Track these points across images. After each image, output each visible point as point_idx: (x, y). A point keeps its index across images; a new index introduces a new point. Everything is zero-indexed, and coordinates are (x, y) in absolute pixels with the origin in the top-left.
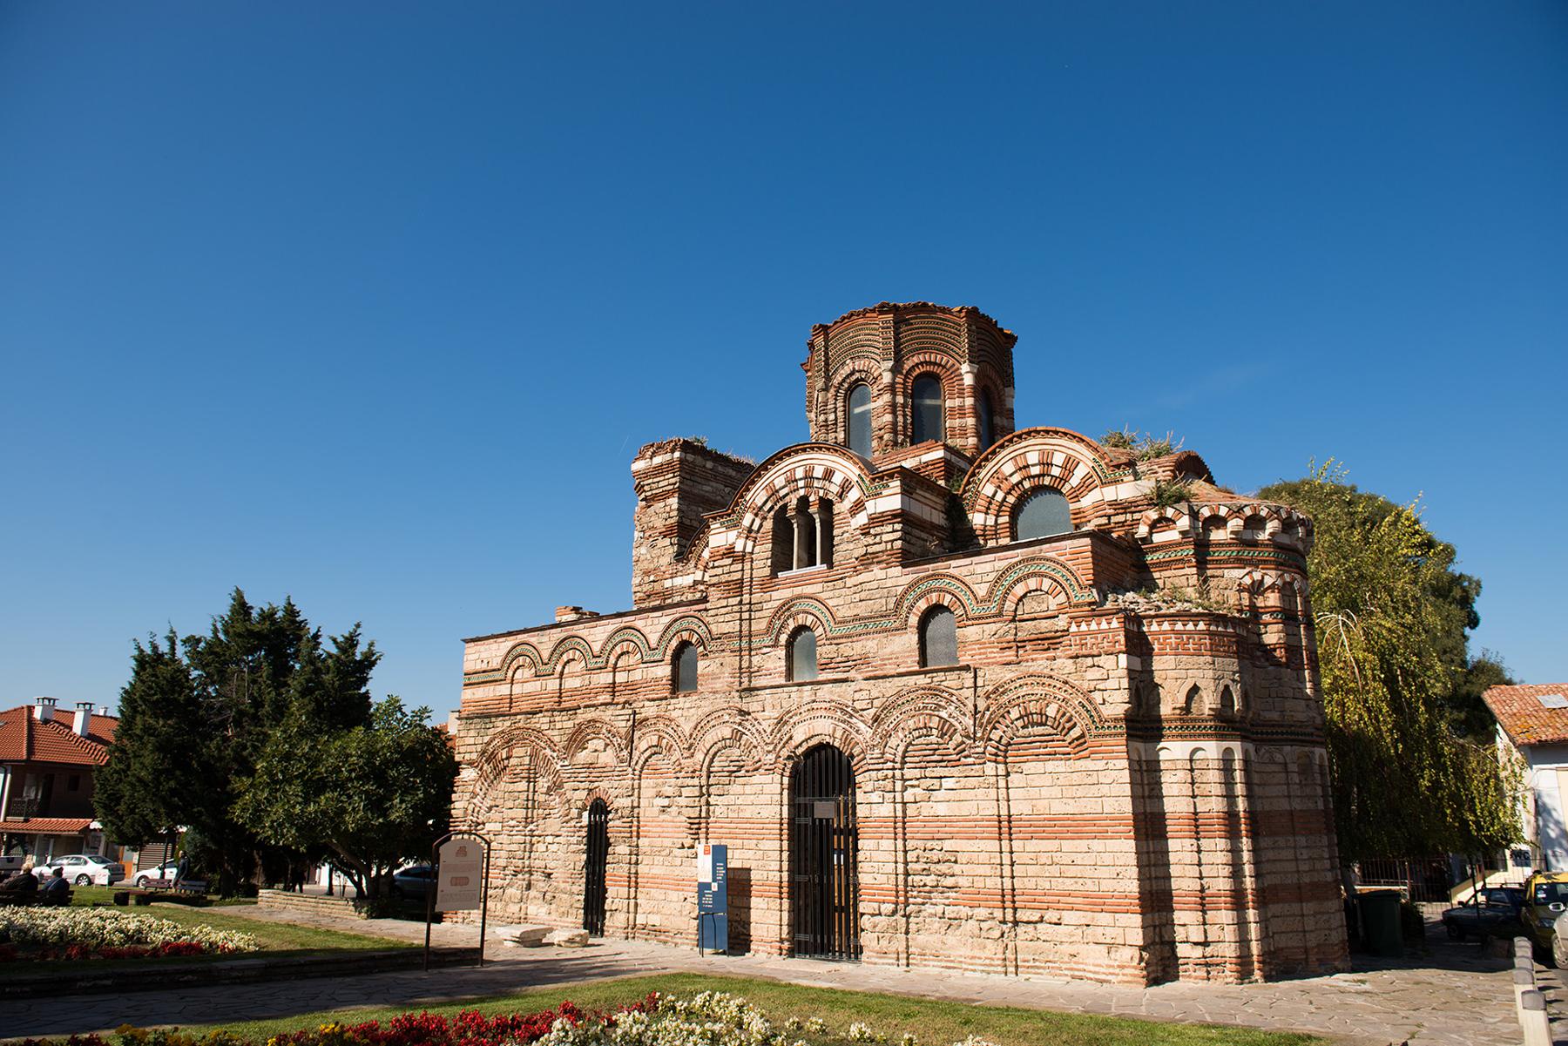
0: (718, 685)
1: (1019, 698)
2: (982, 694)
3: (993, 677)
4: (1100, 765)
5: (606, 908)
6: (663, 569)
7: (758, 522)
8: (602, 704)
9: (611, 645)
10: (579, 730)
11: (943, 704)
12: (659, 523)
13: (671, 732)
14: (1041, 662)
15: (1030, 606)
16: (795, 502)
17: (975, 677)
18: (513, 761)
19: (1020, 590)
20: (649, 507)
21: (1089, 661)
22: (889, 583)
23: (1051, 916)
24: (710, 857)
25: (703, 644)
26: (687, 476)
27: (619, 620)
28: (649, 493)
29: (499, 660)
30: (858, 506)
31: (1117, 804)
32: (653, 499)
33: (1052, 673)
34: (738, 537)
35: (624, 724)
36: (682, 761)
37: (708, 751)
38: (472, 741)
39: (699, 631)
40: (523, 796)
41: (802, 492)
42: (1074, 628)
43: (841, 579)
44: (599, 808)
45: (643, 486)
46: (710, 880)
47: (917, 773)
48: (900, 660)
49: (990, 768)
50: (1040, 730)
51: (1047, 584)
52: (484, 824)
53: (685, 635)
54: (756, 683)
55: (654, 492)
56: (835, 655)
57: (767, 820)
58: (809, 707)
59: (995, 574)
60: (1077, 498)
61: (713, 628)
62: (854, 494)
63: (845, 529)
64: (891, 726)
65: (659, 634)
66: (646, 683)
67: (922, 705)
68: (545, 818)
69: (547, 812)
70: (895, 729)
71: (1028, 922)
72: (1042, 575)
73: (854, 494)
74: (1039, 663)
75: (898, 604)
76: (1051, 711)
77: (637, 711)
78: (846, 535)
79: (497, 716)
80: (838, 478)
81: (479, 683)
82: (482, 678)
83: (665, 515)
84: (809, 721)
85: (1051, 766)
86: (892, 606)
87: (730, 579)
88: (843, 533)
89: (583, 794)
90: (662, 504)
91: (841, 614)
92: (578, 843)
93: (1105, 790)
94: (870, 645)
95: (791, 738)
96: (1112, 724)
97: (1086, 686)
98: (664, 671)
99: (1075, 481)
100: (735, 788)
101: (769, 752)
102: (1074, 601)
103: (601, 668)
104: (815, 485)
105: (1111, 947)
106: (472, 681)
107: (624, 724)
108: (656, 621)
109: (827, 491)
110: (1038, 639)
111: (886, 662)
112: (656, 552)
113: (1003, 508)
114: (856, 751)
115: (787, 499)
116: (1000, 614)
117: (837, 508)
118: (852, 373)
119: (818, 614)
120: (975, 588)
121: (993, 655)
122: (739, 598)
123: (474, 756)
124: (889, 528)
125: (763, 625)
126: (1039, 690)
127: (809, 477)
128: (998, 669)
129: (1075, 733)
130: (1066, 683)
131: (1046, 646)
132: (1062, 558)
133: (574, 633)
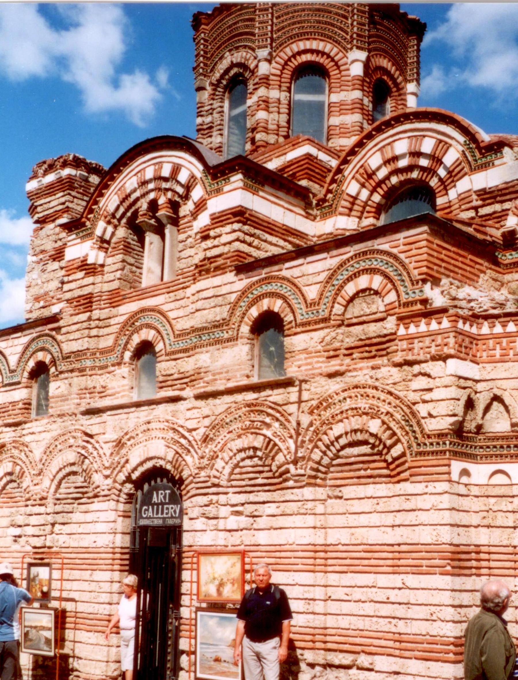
1: (342, 412)
2: (306, 409)
3: (319, 390)
7: (110, 229)
11: (268, 420)
14: (365, 371)
17: (300, 391)
19: (350, 289)
20: (41, 229)
21: (416, 369)
25: (55, 365)
26: (79, 196)
28: (41, 215)
31: (435, 533)
33: (377, 384)
34: (92, 248)
36: (32, 488)
37: (55, 477)
39: (53, 350)
41: (152, 196)
42: (402, 331)
43: (183, 288)
47: (242, 498)
48: (230, 375)
56: (172, 372)
59: (326, 273)
63: (189, 233)
64: (219, 446)
65: (18, 356)
67: (248, 423)
70: (222, 450)
73: (197, 193)
78: (190, 240)
80: (183, 177)
84: (145, 443)
85: (371, 490)
86: (225, 315)
88: (187, 238)
91: (181, 325)
93: (423, 517)
95: (127, 461)
96: (434, 440)
100: (77, 517)
101: (107, 477)
102: (404, 298)
110: (366, 345)
111: (217, 377)
112: (45, 276)
113: (368, 208)
114: (185, 474)
115: (139, 204)
119: (159, 326)
120: (305, 289)
121: (319, 365)
124: (228, 228)
126: (363, 404)
128: (323, 381)
129: (396, 451)
130: (390, 393)
131: (373, 353)
132: (395, 251)
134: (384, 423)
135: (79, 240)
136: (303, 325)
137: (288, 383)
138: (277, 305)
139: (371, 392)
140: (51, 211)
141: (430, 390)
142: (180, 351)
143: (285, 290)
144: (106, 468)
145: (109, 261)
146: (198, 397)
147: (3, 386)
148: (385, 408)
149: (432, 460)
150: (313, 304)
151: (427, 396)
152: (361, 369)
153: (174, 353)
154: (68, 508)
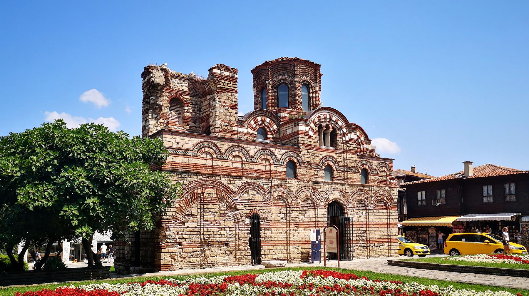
0: (305, 178)
4: (393, 211)
5: (262, 253)
6: (232, 122)
8: (256, 177)
9: (259, 155)
10: (244, 186)
13: (287, 191)
15: (382, 173)
16: (325, 125)
18: (205, 195)
20: (224, 92)
22: (355, 159)
24: (315, 234)
29: (191, 146)
30: (344, 135)
35: (266, 186)
36: (292, 202)
41: (327, 123)
42: (390, 181)
44: (255, 218)
46: (316, 240)
49: (375, 211)
50: (382, 203)
51: (386, 170)
52: (183, 223)
54: (318, 180)
55: (226, 87)
57: (323, 222)
61: (303, 159)
63: (340, 139)
66: (276, 173)
68: (224, 220)
69: (225, 218)
71: (379, 246)
72: (384, 167)
74: (383, 187)
76: (385, 199)
77: (273, 182)
79: (193, 173)
80: (340, 123)
83: (232, 99)
86: (355, 166)
87: (308, 143)
89: (248, 212)
90: (230, 94)
93: (394, 217)
94: (350, 175)
97: (391, 194)
98: (283, 169)
100: (309, 212)
101: (322, 202)
107: (266, 186)
108: (279, 150)
114: (346, 203)
117: (338, 132)
118: (305, 81)
122: (312, 151)
124: (354, 144)
127: (331, 119)
128: (376, 187)
129: (389, 204)
133: (239, 145)
134: (387, 198)
135: (304, 125)
136: (373, 174)
137: (369, 187)
138: (367, 168)
139: (385, 192)
140: (229, 88)
141: (394, 193)
142: (340, 171)
144: (322, 199)
145: (314, 136)
146: (349, 185)
147: (275, 164)
148: (387, 195)
151: (394, 194)
152: (382, 186)
153: (339, 171)
154: (306, 209)
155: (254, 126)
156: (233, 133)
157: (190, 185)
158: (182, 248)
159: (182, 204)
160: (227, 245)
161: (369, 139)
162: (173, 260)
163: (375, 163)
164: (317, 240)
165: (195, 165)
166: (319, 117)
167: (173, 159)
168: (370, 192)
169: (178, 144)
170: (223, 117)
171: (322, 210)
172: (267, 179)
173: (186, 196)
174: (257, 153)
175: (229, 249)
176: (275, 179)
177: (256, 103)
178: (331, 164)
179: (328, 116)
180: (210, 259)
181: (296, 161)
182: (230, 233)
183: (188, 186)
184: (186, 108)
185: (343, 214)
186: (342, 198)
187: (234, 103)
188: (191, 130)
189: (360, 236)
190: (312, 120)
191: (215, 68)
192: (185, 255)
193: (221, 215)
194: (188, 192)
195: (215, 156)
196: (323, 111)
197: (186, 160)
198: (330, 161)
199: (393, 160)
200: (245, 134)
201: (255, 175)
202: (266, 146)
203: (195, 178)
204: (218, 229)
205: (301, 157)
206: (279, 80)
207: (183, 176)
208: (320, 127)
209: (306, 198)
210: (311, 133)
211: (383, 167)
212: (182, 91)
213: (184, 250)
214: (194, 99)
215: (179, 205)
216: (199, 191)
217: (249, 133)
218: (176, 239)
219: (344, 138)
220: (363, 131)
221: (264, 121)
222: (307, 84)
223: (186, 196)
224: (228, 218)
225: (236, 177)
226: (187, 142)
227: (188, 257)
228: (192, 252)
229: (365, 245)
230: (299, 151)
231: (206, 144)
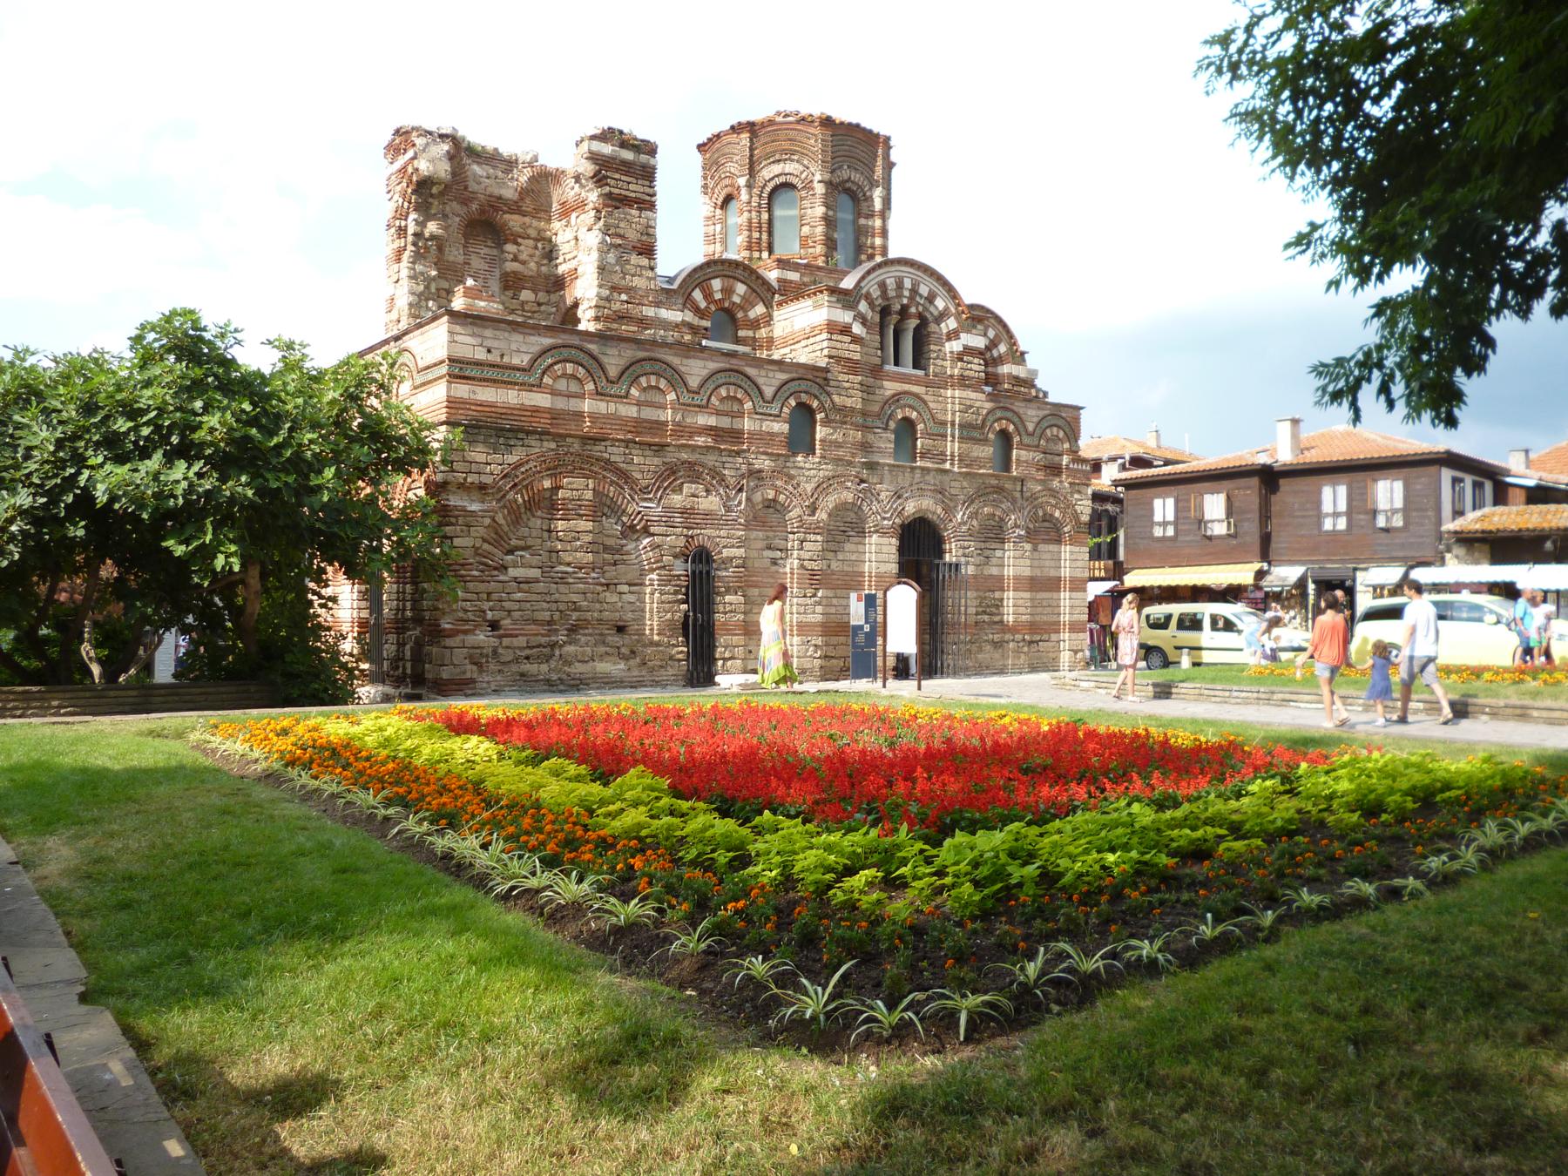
4: (1077, 549)
5: (717, 656)
12: (632, 235)
13: (791, 489)
16: (897, 307)
18: (561, 494)
20: (617, 208)
22: (978, 404)
23: (1045, 637)
27: (723, 358)
28: (616, 191)
30: (953, 335)
32: (621, 201)
38: (481, 458)
40: (589, 538)
41: (905, 301)
44: (701, 559)
45: (606, 177)
46: (862, 622)
49: (1028, 546)
50: (1046, 524)
51: (1061, 434)
53: (804, 397)
55: (623, 192)
58: (916, 487)
60: (996, 366)
61: (836, 398)
62: (952, 324)
68: (615, 564)
70: (976, 513)
72: (1059, 427)
73: (952, 324)
74: (1055, 483)
75: (984, 421)
76: (1057, 514)
79: (528, 433)
80: (940, 304)
81: (485, 380)
82: (490, 374)
89: (681, 542)
90: (635, 212)
91: (940, 417)
92: (676, 593)
98: (781, 427)
99: (995, 353)
100: (848, 546)
101: (884, 519)
103: (699, 406)
104: (918, 299)
105: (1076, 652)
106: (467, 373)
108: (771, 374)
109: (926, 309)
116: (1038, 446)
117: (933, 327)
123: (488, 480)
124: (976, 361)
125: (876, 408)
138: (1011, 428)
140: (633, 195)
143: (1016, 419)
144: (886, 512)
145: (868, 337)
149: (1083, 536)
150: (1032, 435)
155: (703, 305)
156: (643, 322)
157: (521, 465)
158: (500, 637)
159: (500, 518)
160: (621, 629)
161: (1022, 348)
162: (475, 668)
163: (1032, 415)
164: (866, 622)
165: (536, 410)
166: (883, 286)
167: (474, 393)
168: (1018, 495)
169: (489, 351)
170: (616, 279)
171: (885, 540)
172: (738, 453)
173: (511, 496)
174: (710, 381)
175: (627, 638)
176: (759, 452)
177: (710, 239)
178: (914, 415)
179: (908, 284)
180: (578, 668)
181: (815, 404)
182: (632, 598)
183: (516, 468)
184: (510, 247)
185: (940, 553)
186: (939, 510)
187: (644, 238)
188: (523, 310)
189: (984, 612)
190: (864, 291)
191: (593, 138)
192: (507, 656)
193: (606, 548)
194: (515, 485)
195: (590, 386)
196: (893, 268)
197: (512, 397)
198: (910, 407)
199: (1082, 408)
200: (677, 326)
201: (700, 440)
202: (734, 361)
203: (538, 447)
204: (600, 588)
205: (829, 394)
206: (777, 176)
207: (502, 440)
208: (885, 312)
209: (842, 508)
210: (857, 329)
211: (1055, 429)
212: (500, 198)
213: (506, 641)
214: (535, 223)
215: (494, 520)
216: (547, 484)
217: (690, 326)
218: (484, 612)
219: (947, 345)
220: (1005, 326)
221: (728, 292)
222: (853, 191)
223: (511, 496)
224: (625, 557)
225: (650, 445)
226: (514, 347)
227: (517, 660)
228: (528, 647)
229: (996, 637)
230: (826, 379)
231: (565, 353)
